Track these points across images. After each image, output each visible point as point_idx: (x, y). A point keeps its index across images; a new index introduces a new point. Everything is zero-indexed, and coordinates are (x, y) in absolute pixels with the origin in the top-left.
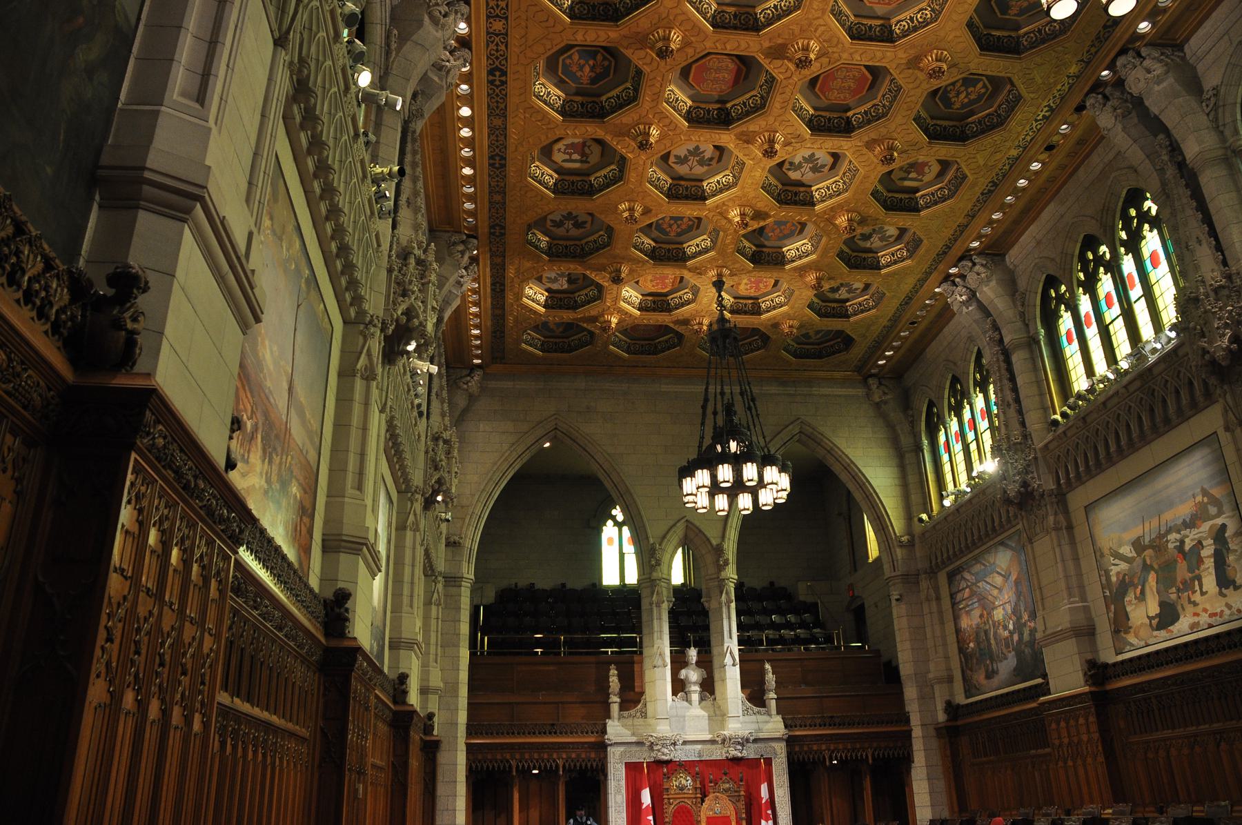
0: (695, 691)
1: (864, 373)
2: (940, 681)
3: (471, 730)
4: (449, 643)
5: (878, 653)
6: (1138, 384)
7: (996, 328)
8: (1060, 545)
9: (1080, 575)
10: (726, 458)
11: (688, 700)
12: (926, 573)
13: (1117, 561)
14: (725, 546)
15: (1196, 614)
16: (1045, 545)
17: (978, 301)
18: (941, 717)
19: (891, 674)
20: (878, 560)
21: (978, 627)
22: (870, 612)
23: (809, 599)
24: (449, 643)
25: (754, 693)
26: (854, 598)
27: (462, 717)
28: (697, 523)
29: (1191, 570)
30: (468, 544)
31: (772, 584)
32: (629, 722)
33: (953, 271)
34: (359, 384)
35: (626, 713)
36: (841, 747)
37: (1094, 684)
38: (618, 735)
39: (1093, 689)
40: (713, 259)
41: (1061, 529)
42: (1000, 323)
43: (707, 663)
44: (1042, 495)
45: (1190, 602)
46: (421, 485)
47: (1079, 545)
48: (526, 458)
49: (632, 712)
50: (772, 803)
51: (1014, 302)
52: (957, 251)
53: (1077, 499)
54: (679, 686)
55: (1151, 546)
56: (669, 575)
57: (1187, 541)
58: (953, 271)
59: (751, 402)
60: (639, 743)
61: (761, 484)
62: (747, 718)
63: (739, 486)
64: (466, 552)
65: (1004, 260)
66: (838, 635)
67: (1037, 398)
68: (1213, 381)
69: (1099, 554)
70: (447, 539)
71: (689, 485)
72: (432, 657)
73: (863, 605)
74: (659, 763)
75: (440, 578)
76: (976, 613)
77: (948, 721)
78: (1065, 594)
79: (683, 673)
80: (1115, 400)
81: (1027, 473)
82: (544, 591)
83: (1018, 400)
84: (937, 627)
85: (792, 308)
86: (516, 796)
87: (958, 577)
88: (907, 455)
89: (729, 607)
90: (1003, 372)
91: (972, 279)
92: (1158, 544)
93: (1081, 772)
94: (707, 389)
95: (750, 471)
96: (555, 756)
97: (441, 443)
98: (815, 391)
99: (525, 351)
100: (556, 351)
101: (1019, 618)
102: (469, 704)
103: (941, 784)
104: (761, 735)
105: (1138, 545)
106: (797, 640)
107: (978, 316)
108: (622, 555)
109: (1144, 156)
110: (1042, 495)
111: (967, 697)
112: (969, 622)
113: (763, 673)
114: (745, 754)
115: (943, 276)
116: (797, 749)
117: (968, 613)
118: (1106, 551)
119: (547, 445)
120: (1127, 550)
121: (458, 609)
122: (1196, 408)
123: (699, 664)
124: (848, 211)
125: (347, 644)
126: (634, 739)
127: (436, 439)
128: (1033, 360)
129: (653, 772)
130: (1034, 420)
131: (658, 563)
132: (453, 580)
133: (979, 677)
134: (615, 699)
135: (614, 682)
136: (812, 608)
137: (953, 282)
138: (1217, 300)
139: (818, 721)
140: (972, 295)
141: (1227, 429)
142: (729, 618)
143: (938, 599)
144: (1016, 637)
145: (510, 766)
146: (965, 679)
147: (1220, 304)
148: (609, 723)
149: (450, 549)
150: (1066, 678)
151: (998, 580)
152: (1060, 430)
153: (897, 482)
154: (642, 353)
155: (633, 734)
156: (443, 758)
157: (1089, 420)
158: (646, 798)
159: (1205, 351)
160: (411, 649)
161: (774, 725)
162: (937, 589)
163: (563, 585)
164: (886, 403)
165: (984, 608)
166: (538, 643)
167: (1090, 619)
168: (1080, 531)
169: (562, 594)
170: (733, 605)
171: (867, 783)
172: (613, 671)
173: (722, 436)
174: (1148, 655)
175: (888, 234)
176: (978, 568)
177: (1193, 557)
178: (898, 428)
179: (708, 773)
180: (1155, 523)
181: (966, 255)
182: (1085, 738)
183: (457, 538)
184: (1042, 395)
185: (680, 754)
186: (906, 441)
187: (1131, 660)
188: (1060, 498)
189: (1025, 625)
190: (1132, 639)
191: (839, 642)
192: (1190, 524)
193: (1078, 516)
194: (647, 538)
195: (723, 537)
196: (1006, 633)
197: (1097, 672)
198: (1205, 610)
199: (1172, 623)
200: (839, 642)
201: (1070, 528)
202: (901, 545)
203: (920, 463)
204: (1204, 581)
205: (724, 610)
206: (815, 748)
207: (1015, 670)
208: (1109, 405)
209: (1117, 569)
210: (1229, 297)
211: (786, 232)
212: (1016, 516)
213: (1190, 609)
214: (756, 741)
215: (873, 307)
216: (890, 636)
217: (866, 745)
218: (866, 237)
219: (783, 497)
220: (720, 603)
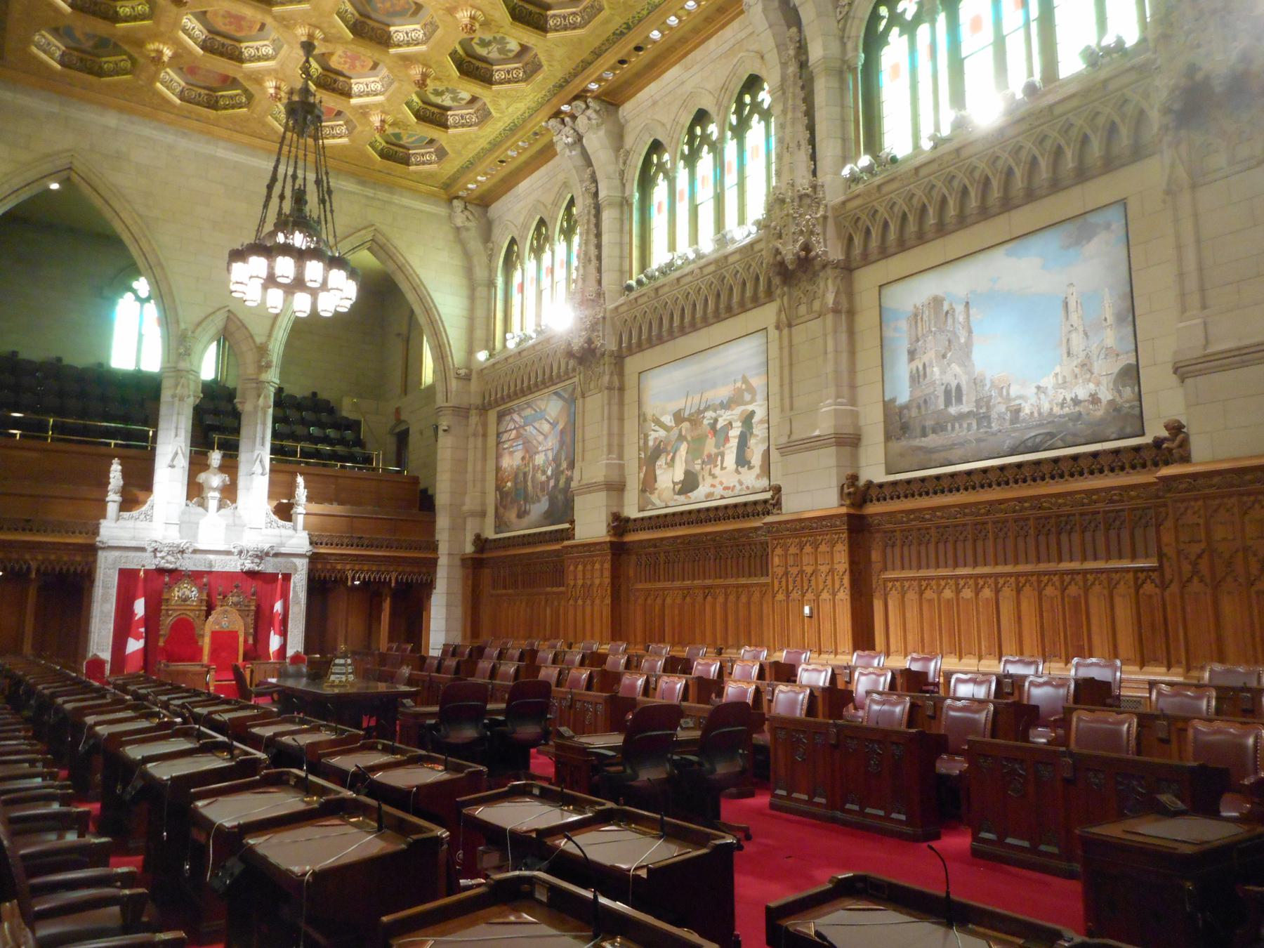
0: (213, 498)
1: (449, 192)
2: (472, 514)
5: (415, 480)
6: (712, 268)
7: (594, 180)
8: (609, 404)
9: (621, 435)
10: (287, 250)
11: (203, 504)
13: (657, 428)
14: (271, 347)
15: (713, 486)
16: (595, 404)
17: (583, 147)
18: (469, 549)
19: (426, 502)
20: (431, 388)
21: (518, 468)
22: (413, 439)
23: (352, 416)
26: (399, 421)
28: (241, 316)
29: (717, 446)
31: (314, 394)
32: (130, 524)
33: (565, 108)
35: (126, 514)
37: (615, 535)
39: (614, 539)
40: (305, 12)
41: (613, 389)
42: (599, 176)
43: (230, 466)
44: (603, 355)
45: (710, 474)
47: (626, 408)
48: (24, 195)
49: (135, 513)
51: (617, 157)
52: (574, 88)
53: (633, 364)
54: (195, 491)
55: (689, 420)
56: (199, 367)
57: (720, 420)
58: (565, 108)
59: (326, 195)
65: (617, 111)
67: (617, 260)
68: (777, 281)
69: (642, 418)
71: (239, 270)
73: (407, 430)
74: (161, 571)
76: (519, 455)
78: (605, 449)
79: (202, 477)
80: (689, 278)
81: (593, 330)
82: (30, 362)
83: (599, 258)
84: (479, 464)
85: (388, 99)
87: (508, 418)
88: (479, 289)
89: (265, 413)
90: (592, 226)
91: (582, 122)
92: (695, 420)
93: (588, 610)
94: (276, 168)
95: (314, 269)
96: (27, 556)
98: (396, 199)
99: (35, 58)
100: (81, 70)
101: (558, 465)
103: (458, 612)
104: (283, 550)
105: (678, 417)
106: (335, 456)
107: (580, 162)
108: (140, 336)
109: (773, 45)
110: (603, 355)
111: (496, 533)
112: (510, 462)
115: (555, 110)
116: (319, 566)
117: (511, 453)
118: (649, 417)
119: (55, 186)
120: (668, 420)
122: (756, 302)
123: (222, 468)
124: (473, 7)
128: (622, 221)
129: (151, 583)
130: (610, 280)
131: (188, 353)
133: (512, 515)
134: (113, 498)
136: (354, 425)
137: (563, 120)
138: (800, 206)
139: (346, 541)
140: (579, 138)
141: (778, 327)
142: (264, 424)
143: (485, 435)
144: (552, 483)
146: (497, 515)
147: (802, 211)
150: (591, 525)
151: (546, 427)
152: (633, 295)
153: (465, 313)
154: (198, 104)
157: (661, 292)
158: (139, 607)
159: (778, 252)
162: (485, 425)
164: (467, 229)
165: (527, 451)
166: (17, 424)
167: (623, 476)
168: (630, 395)
169: (55, 370)
170: (271, 411)
171: (387, 606)
173: (284, 224)
174: (666, 515)
175: (509, 47)
176: (528, 412)
177: (721, 434)
178: (475, 260)
179: (215, 587)
180: (697, 400)
181: (581, 96)
182: (597, 582)
184: (621, 257)
186: (480, 274)
187: (650, 518)
188: (619, 360)
189: (562, 472)
190: (654, 498)
191: (378, 464)
192: (726, 406)
193: (630, 380)
194: (177, 322)
195: (270, 336)
196: (544, 478)
197: (620, 524)
198: (721, 483)
199: (692, 490)
200: (378, 464)
201: (622, 389)
202: (458, 377)
203: (490, 300)
204: (726, 458)
205: (260, 414)
206: (339, 567)
207: (546, 512)
208: (683, 281)
209: (656, 434)
210: (810, 206)
211: (398, 8)
212: (574, 370)
213: (709, 480)
214: (276, 555)
215: (476, 124)
216: (431, 466)
218: (484, 43)
219: (345, 307)
220: (256, 407)
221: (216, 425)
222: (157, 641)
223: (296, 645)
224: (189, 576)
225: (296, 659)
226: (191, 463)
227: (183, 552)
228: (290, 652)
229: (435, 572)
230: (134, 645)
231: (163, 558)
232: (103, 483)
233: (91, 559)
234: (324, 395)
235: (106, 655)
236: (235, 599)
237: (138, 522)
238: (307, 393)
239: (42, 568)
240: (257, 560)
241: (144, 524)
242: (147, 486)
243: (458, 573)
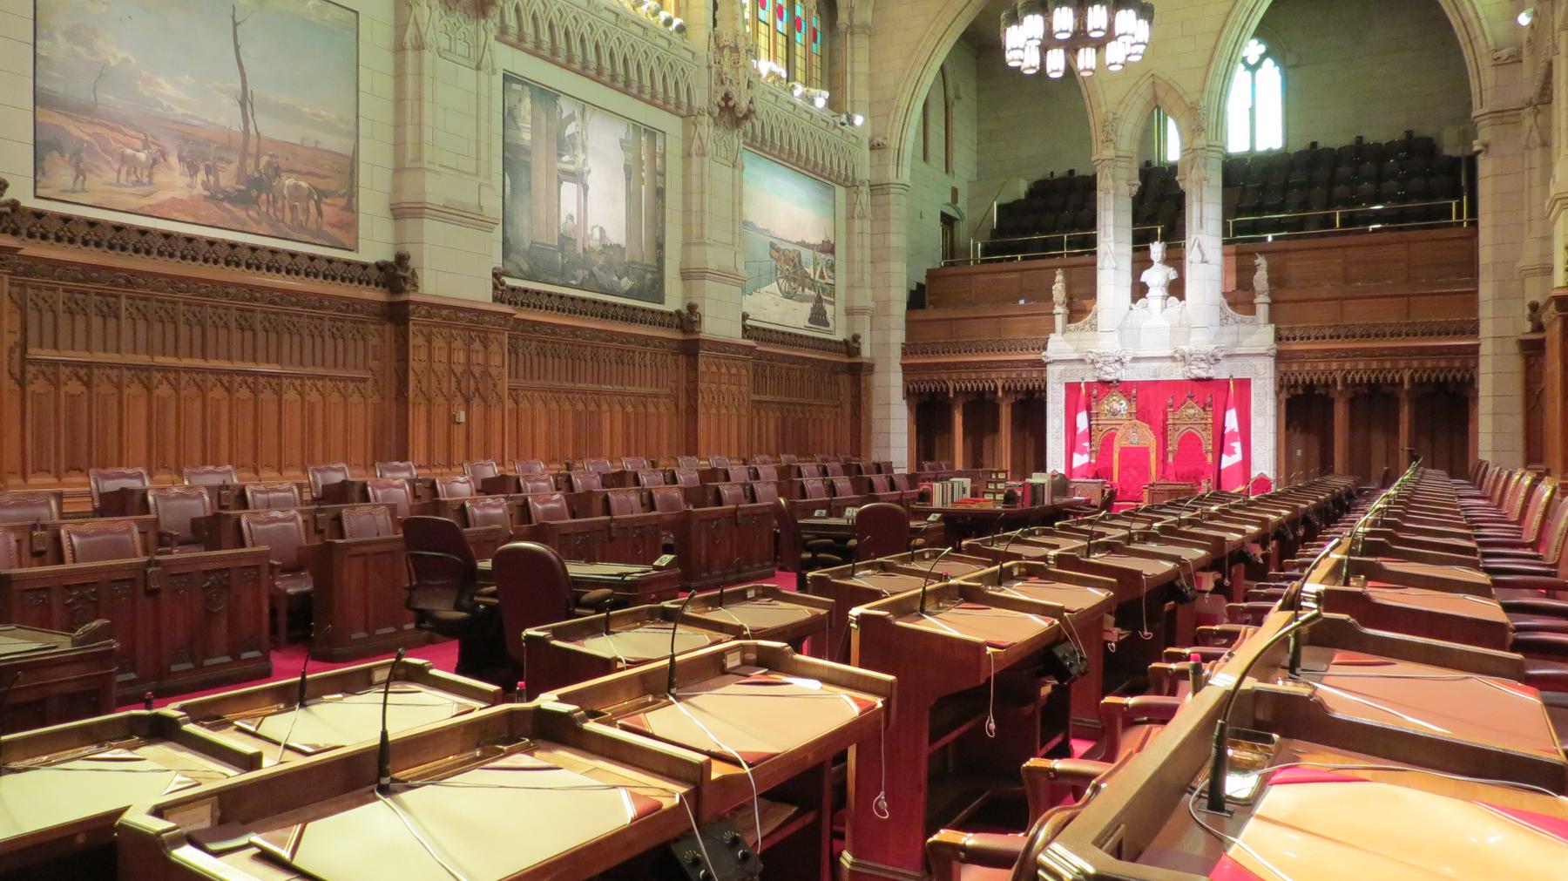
3: (907, 350)
4: (879, 257)
12: (1530, 104)
14: (1202, 104)
18: (1528, 326)
24: (879, 257)
25: (1239, 298)
27: (898, 337)
30: (894, 143)
31: (1409, 133)
34: (410, 56)
35: (1072, 326)
36: (1361, 366)
43: (1175, 258)
46: (705, 105)
49: (1080, 324)
54: (1140, 291)
60: (1082, 361)
61: (1110, 35)
63: (1079, 38)
64: (892, 154)
66: (1460, 207)
70: (871, 141)
72: (857, 276)
75: (865, 189)
77: (1533, 331)
86: (958, 419)
96: (994, 376)
97: (726, 52)
102: (907, 321)
103: (1516, 422)
104: (1238, 350)
113: (1254, 269)
114: (1213, 373)
116: (1295, 367)
121: (887, 219)
125: (403, 298)
126: (1076, 356)
127: (720, 49)
132: (879, 188)
134: (1060, 310)
135: (1058, 290)
139: (1328, 332)
148: (1052, 336)
149: (876, 152)
155: (1076, 350)
156: (877, 379)
160: (703, 278)
161: (1261, 336)
163: (1071, 172)
166: (1377, 218)
172: (1059, 277)
183: (880, 140)
191: (1460, 215)
200: (1460, 215)
202: (1498, 63)
206: (1322, 366)
217: (1402, 364)
221: (1159, 210)
223: (1264, 463)
225: (1263, 483)
226: (1134, 262)
227: (1120, 361)
228: (1255, 474)
229: (1477, 365)
232: (1049, 296)
234: (1428, 131)
235: (1062, 470)
238: (1398, 136)
240: (1202, 365)
242: (1092, 295)
243: (1515, 364)
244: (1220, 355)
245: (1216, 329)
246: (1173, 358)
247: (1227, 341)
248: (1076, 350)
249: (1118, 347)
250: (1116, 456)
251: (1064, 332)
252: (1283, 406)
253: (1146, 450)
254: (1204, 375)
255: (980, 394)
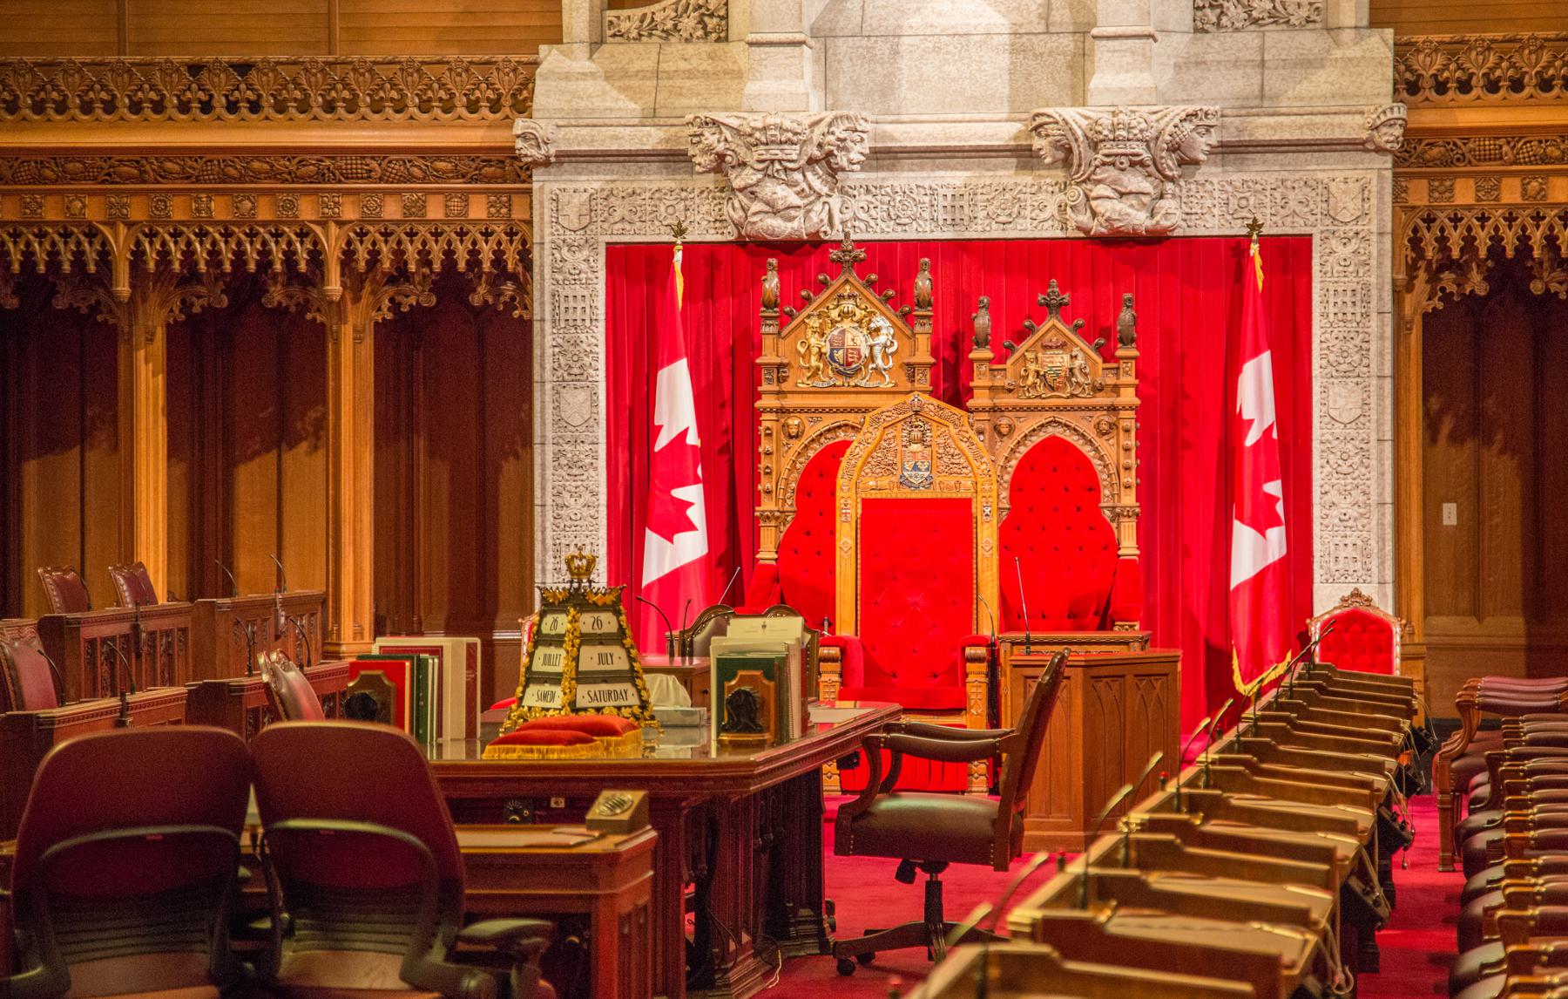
32: (641, 57)
38: (576, 120)
50: (1292, 446)
60: (674, 158)
62: (1219, 45)
74: (756, 249)
96: (307, 211)
104: (1263, 128)
116: (1464, 193)
126: (652, 138)
145: (105, 256)
148: (550, 57)
155: (651, 116)
185: (861, 214)
214: (1231, 151)
222: (755, 545)
223: (1356, 555)
224: (862, 268)
230: (674, 553)
231: (751, 192)
233: (518, 214)
236: (1060, 360)
237: (675, 47)
239: (362, 254)
240: (1136, 181)
241: (697, 54)
244: (1202, 144)
245: (1179, 43)
246: (1024, 156)
247: (1221, 89)
248: (651, 116)
249: (815, 107)
250: (846, 538)
251: (596, 44)
252: (1415, 338)
253: (958, 513)
254: (1139, 220)
255: (246, 285)
